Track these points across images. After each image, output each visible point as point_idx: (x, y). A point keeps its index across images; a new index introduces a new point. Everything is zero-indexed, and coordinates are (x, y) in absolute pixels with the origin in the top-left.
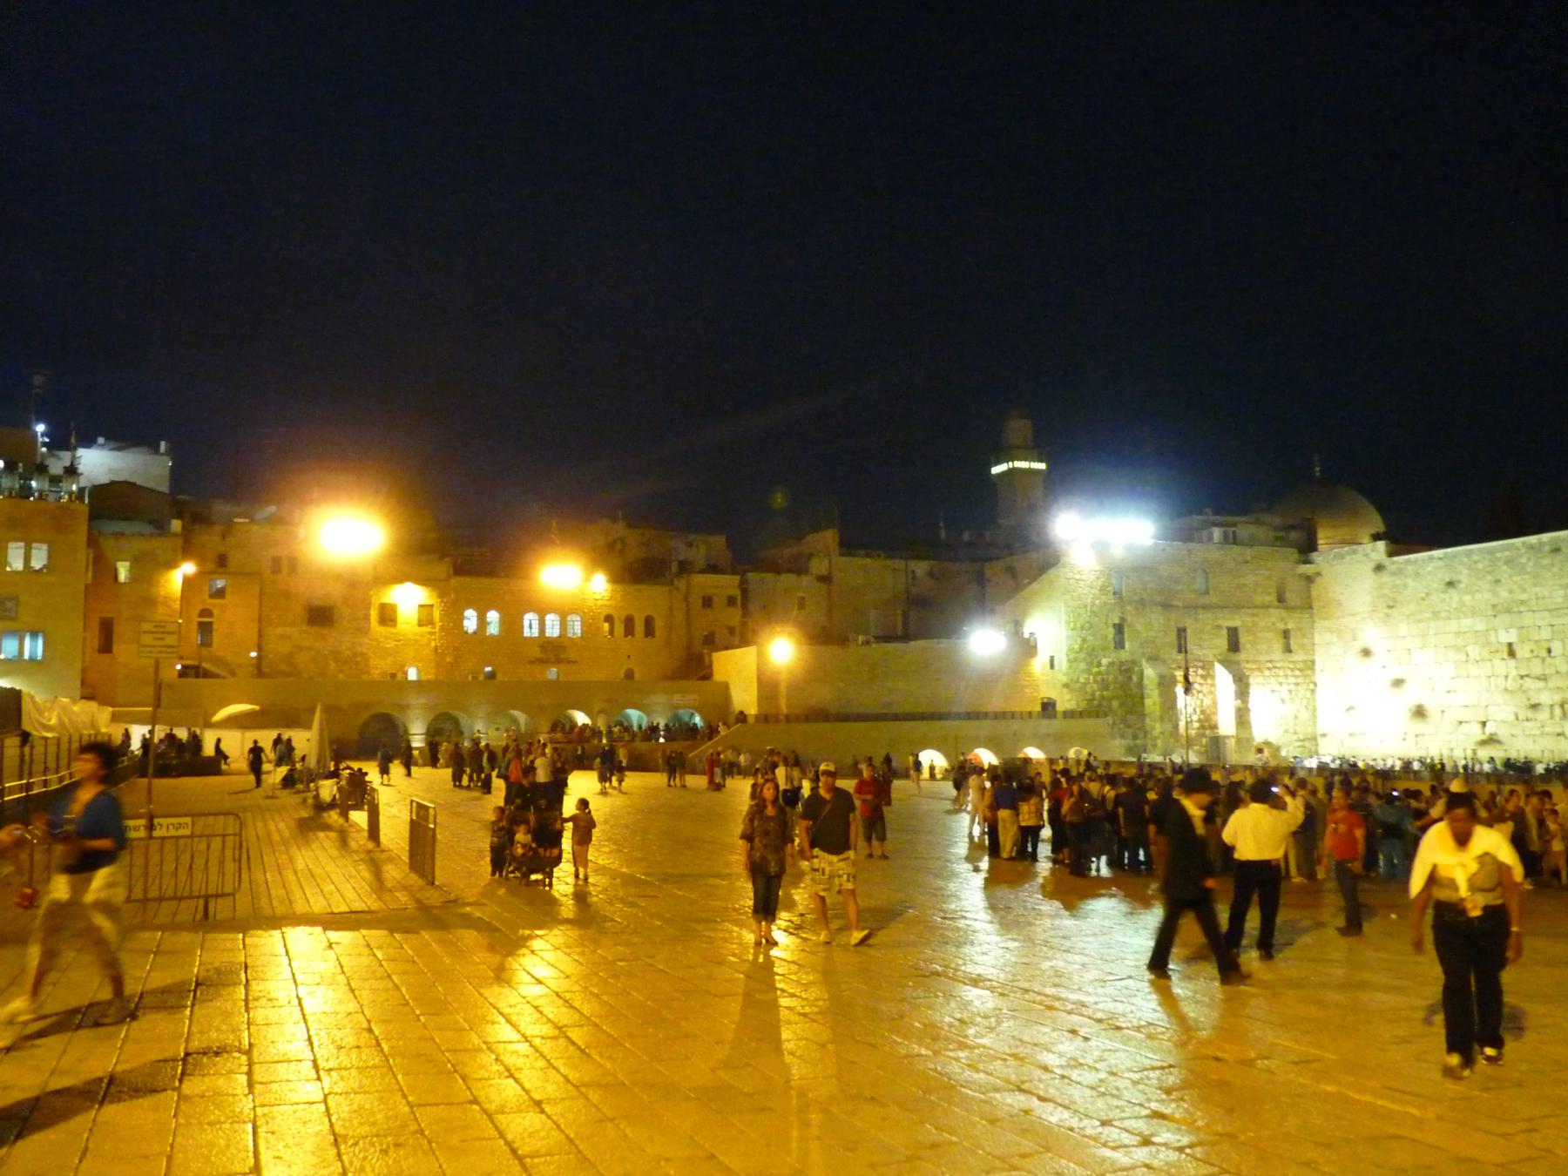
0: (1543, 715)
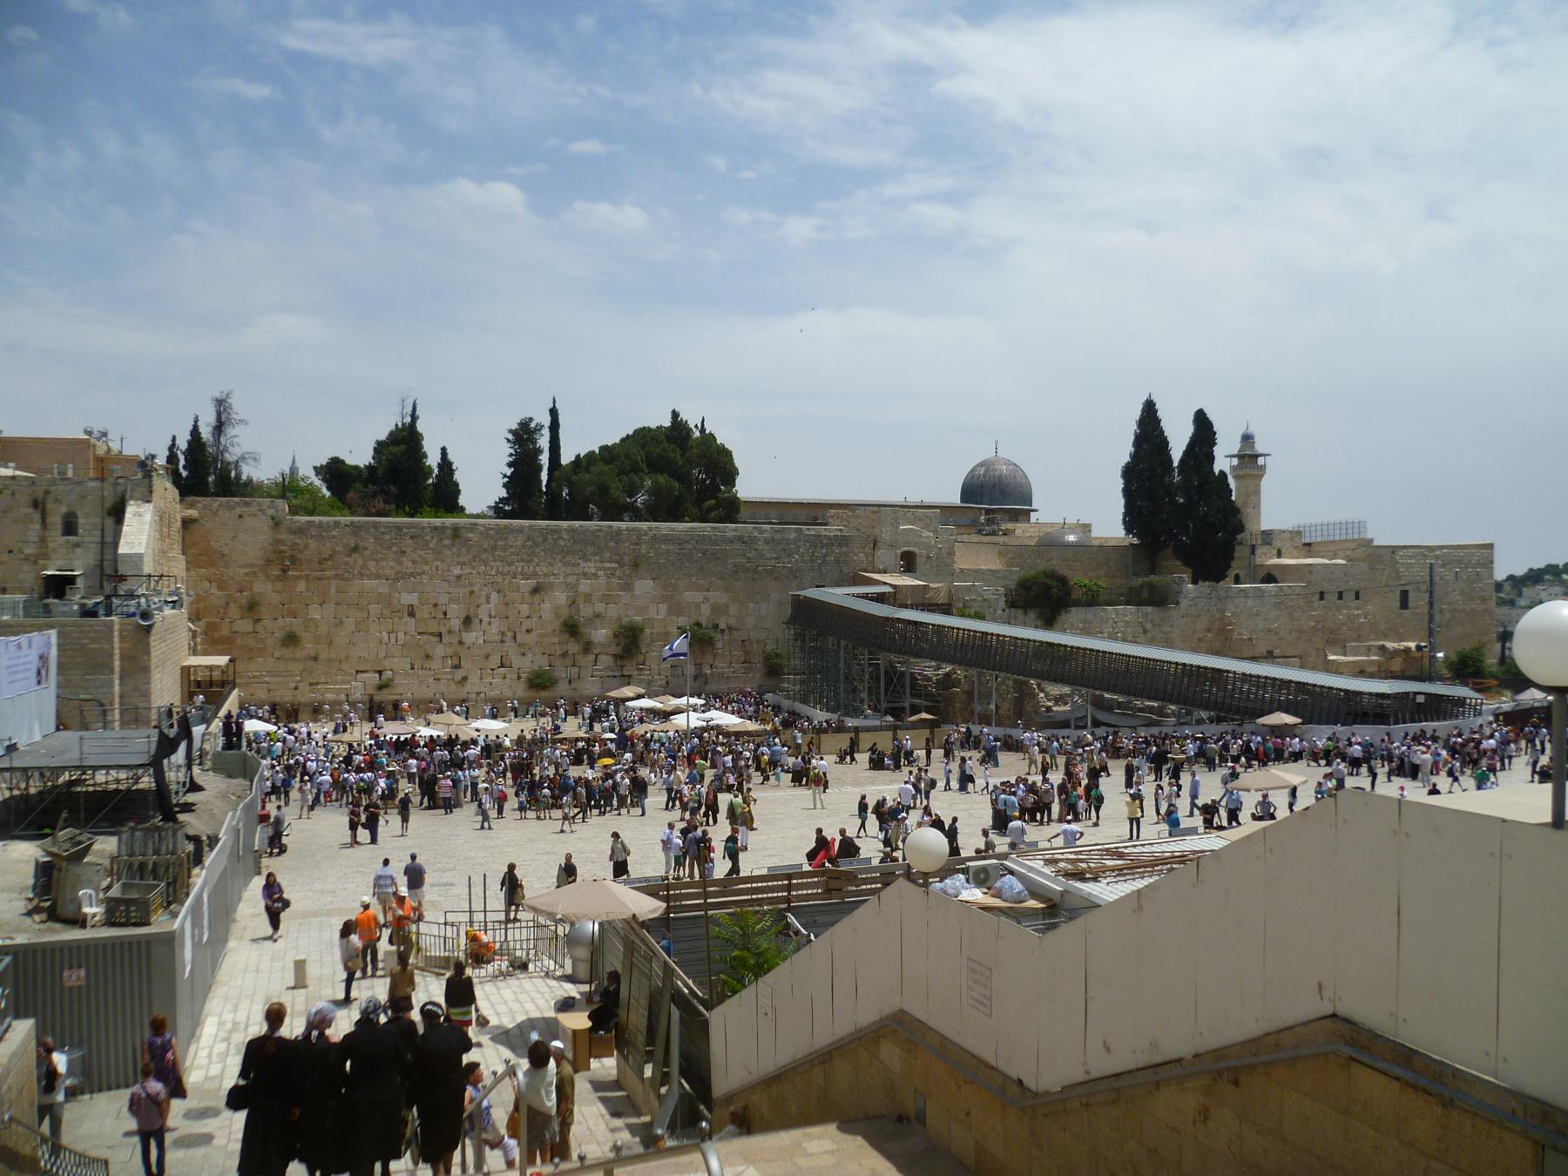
0: (435, 664)
